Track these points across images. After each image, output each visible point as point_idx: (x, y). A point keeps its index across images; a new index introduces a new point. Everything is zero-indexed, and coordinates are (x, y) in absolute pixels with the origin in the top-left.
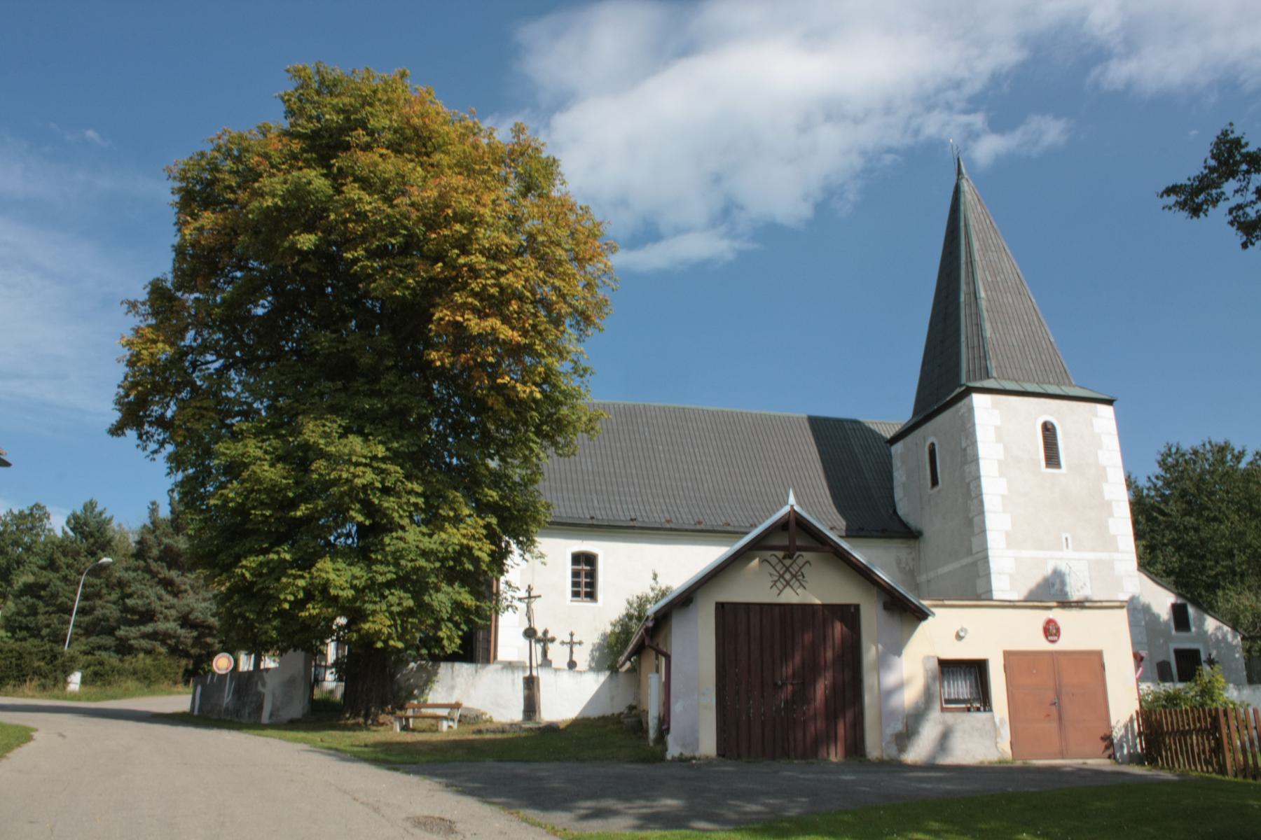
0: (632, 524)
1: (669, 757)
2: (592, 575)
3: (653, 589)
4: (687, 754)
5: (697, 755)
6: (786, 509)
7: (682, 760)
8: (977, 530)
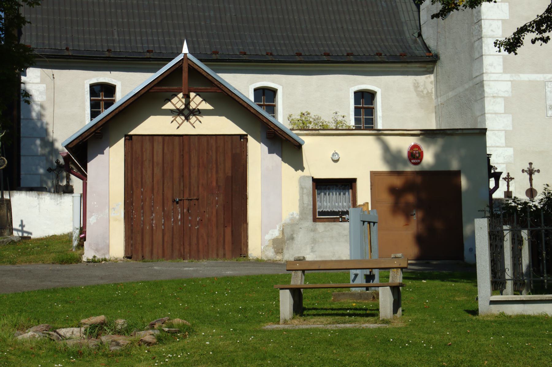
0: (148, 55)
1: (84, 259)
4: (99, 256)
5: (107, 257)
6: (180, 57)
7: (94, 261)
8: (477, 55)
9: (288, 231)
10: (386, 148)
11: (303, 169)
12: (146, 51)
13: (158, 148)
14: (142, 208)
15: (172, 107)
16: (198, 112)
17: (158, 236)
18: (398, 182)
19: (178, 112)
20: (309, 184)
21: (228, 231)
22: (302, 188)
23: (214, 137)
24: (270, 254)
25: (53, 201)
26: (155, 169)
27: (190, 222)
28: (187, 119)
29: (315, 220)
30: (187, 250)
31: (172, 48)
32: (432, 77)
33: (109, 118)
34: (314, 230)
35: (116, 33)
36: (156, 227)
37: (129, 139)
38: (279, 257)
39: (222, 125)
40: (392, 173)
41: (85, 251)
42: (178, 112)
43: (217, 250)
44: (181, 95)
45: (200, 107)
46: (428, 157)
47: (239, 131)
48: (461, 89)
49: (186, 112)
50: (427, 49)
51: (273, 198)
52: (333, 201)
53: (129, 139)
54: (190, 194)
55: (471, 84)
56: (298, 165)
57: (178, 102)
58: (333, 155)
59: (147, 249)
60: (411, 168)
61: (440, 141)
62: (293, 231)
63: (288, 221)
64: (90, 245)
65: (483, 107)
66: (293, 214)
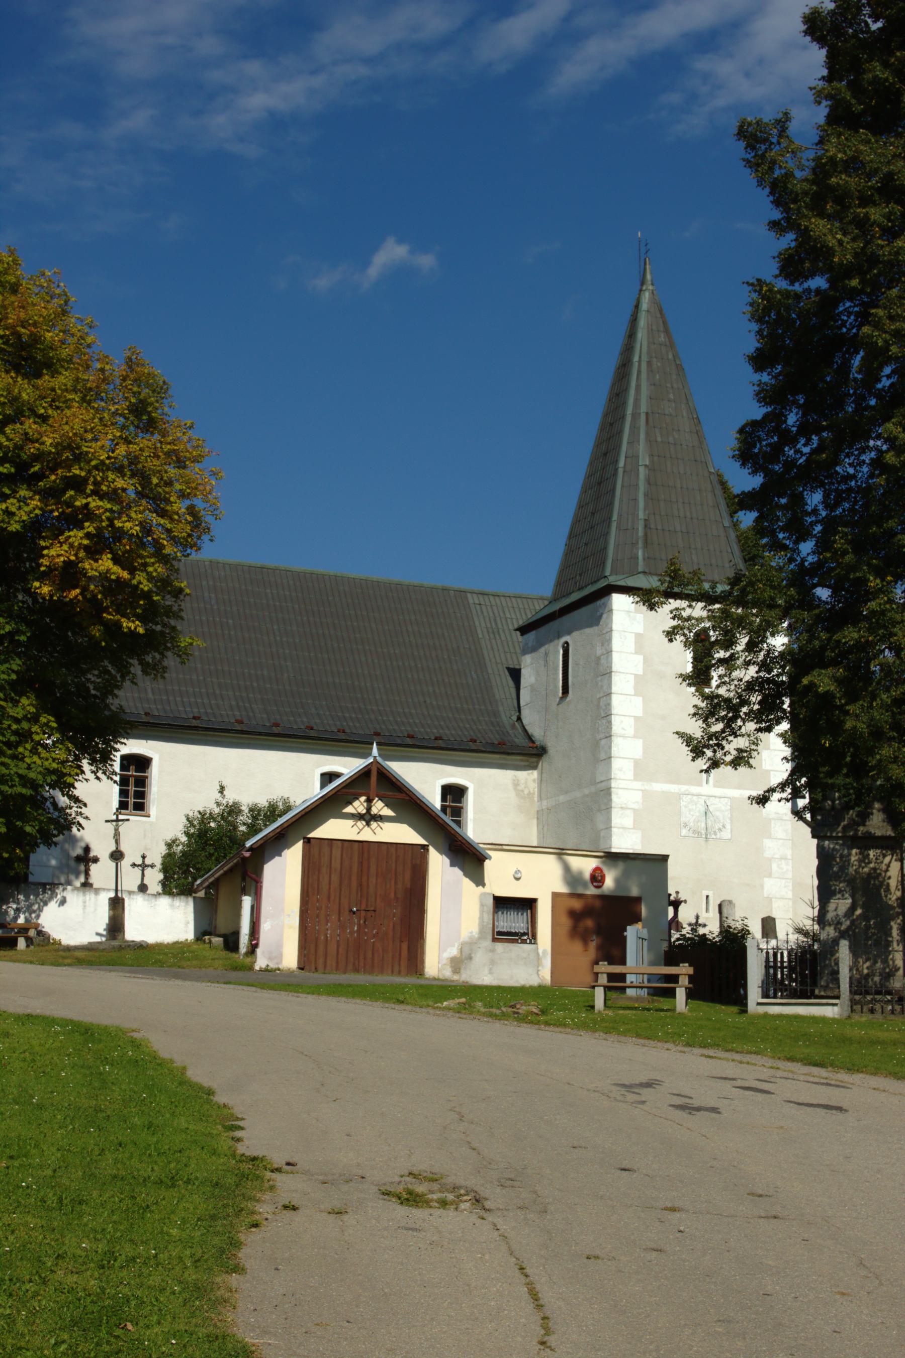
0: (195, 723)
1: (257, 968)
2: (142, 782)
3: (218, 804)
4: (272, 965)
5: (281, 967)
7: (267, 970)
8: (603, 756)
9: (466, 951)
10: (567, 868)
11: (484, 885)
12: (191, 716)
13: (337, 853)
14: (318, 916)
15: (353, 811)
16: (379, 818)
17: (333, 948)
18: (577, 905)
19: (359, 817)
20: (490, 902)
21: (405, 946)
22: (482, 905)
23: (386, 846)
24: (447, 973)
25: (146, 903)
26: (333, 876)
27: (366, 934)
28: (368, 824)
29: (494, 940)
30: (362, 964)
31: (221, 715)
32: (534, 774)
33: (294, 819)
34: (493, 951)
35: (149, 690)
36: (331, 937)
37: (308, 841)
38: (456, 977)
39: (402, 833)
40: (573, 895)
41: (258, 959)
42: (359, 817)
43: (393, 966)
44: (363, 799)
45: (382, 813)
46: (609, 882)
47: (420, 840)
48: (577, 794)
49: (367, 817)
50: (530, 738)
51: (453, 912)
52: (515, 921)
53: (308, 841)
54: (367, 905)
55: (593, 789)
56: (479, 880)
57: (359, 806)
58: (516, 872)
59: (321, 962)
60: (592, 891)
61: (621, 865)
62: (471, 950)
63: (467, 939)
64: (263, 953)
65: (609, 820)
66: (472, 933)
